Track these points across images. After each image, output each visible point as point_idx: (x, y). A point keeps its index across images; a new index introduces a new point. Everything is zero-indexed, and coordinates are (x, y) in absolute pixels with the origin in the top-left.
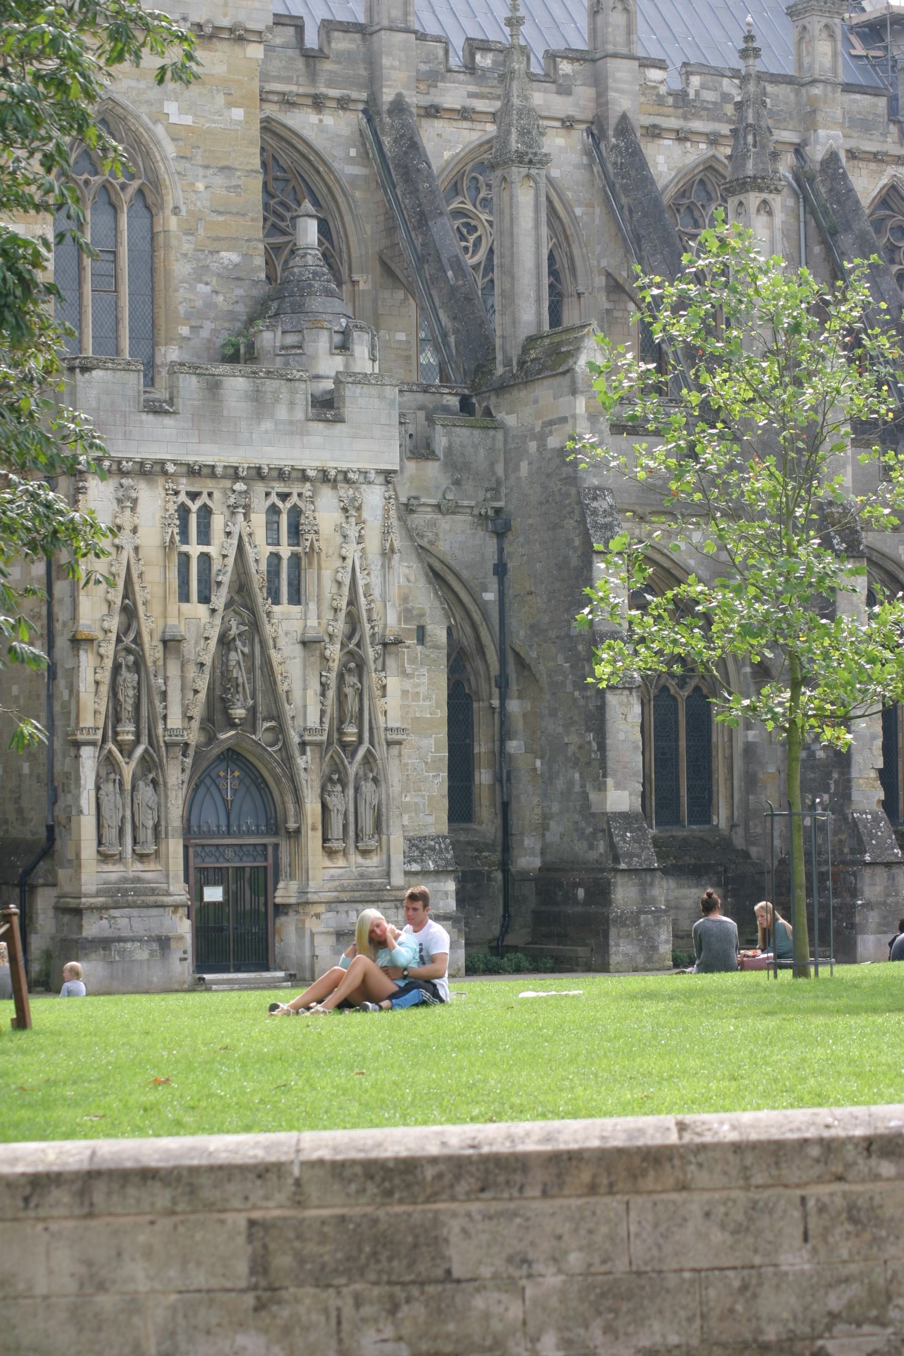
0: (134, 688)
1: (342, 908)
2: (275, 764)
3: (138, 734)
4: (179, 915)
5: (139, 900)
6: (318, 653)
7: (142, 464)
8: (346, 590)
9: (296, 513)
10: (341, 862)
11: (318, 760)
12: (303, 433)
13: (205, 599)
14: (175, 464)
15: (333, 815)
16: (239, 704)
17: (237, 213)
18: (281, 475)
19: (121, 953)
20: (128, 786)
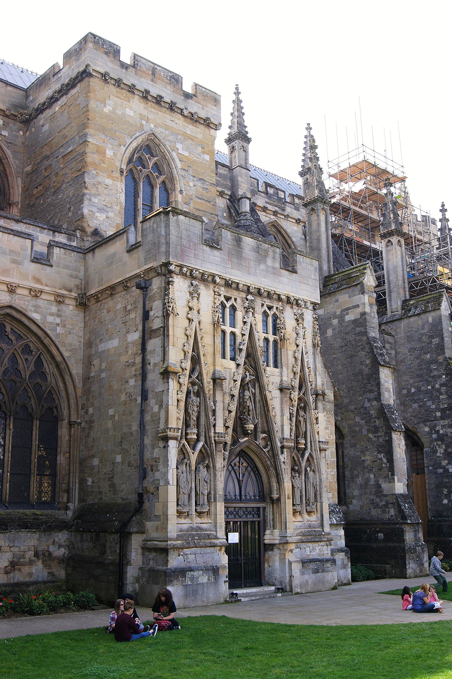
0: (197, 407)
3: (198, 435)
5: (202, 543)
7: (203, 274)
9: (275, 318)
12: (279, 275)
13: (233, 359)
14: (220, 278)
17: (207, 201)
18: (269, 295)
19: (192, 579)
20: (193, 468)
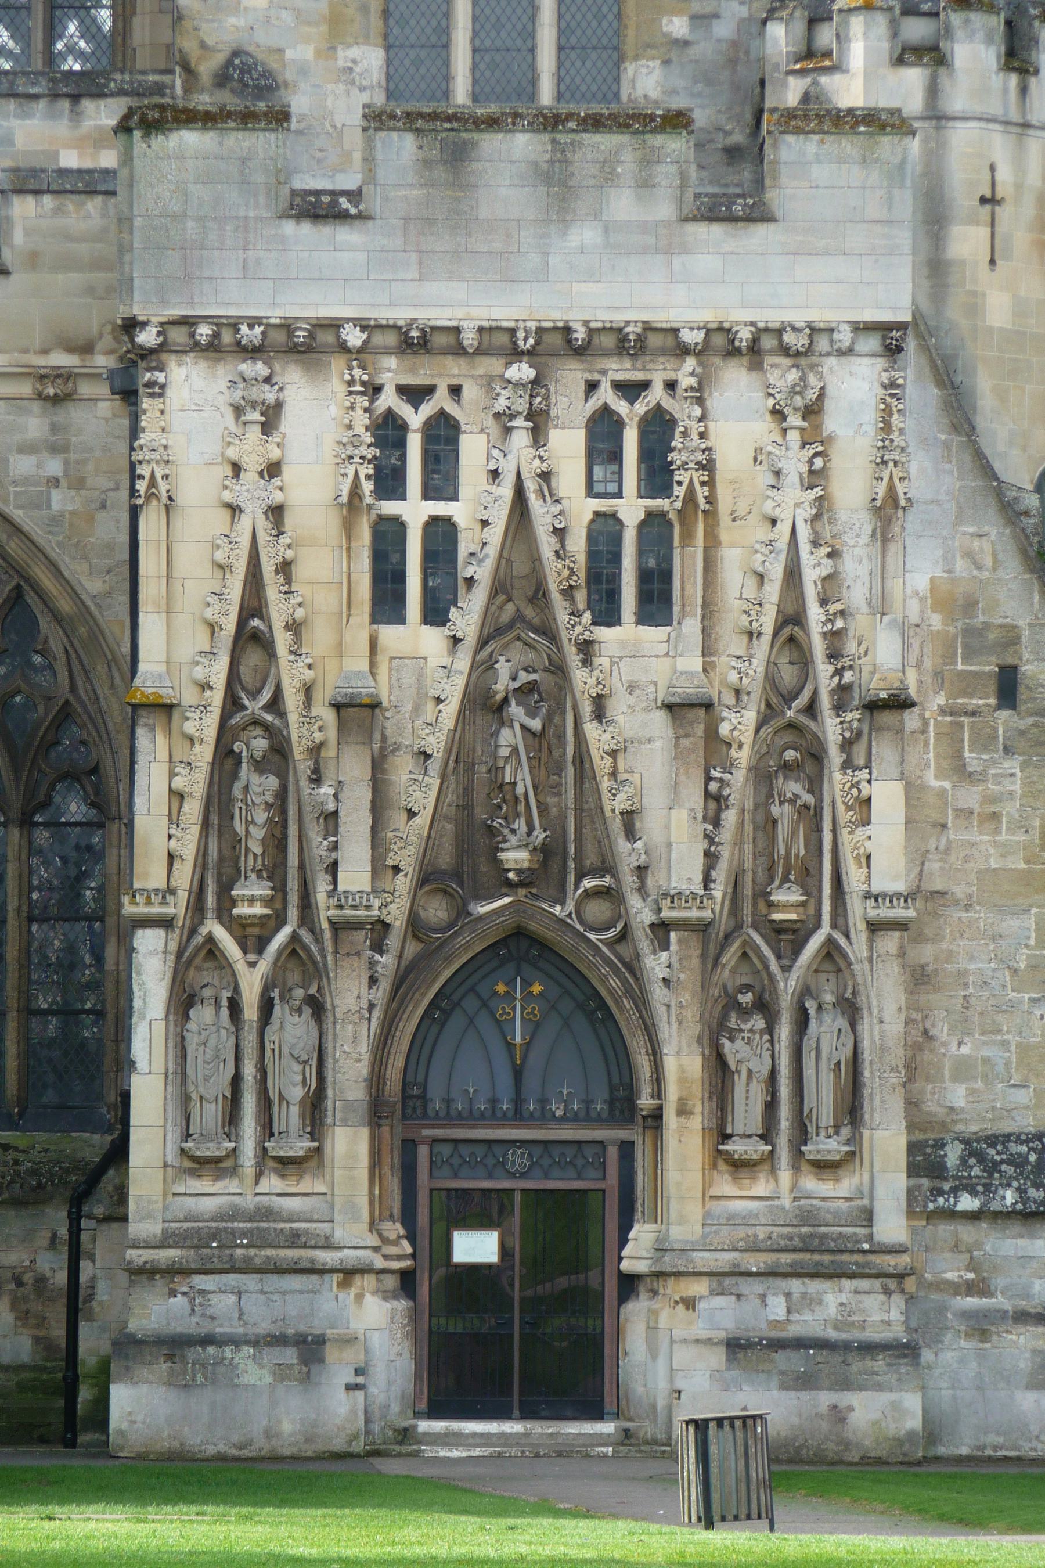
0: (269, 806)
1: (752, 1288)
2: (605, 970)
4: (353, 1291)
6: (700, 730)
7: (287, 326)
8: (773, 591)
10: (761, 1187)
11: (696, 962)
14: (364, 328)
15: (740, 1083)
16: (513, 840)
20: (251, 1013)
